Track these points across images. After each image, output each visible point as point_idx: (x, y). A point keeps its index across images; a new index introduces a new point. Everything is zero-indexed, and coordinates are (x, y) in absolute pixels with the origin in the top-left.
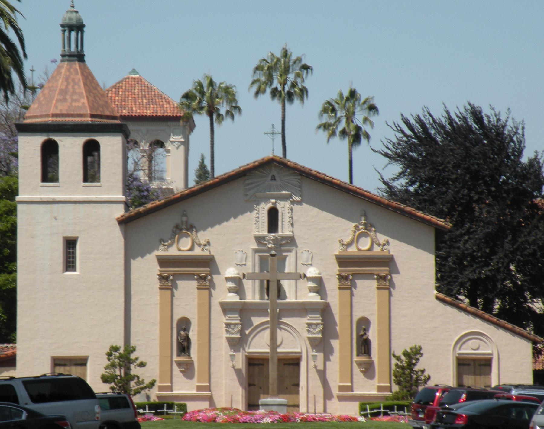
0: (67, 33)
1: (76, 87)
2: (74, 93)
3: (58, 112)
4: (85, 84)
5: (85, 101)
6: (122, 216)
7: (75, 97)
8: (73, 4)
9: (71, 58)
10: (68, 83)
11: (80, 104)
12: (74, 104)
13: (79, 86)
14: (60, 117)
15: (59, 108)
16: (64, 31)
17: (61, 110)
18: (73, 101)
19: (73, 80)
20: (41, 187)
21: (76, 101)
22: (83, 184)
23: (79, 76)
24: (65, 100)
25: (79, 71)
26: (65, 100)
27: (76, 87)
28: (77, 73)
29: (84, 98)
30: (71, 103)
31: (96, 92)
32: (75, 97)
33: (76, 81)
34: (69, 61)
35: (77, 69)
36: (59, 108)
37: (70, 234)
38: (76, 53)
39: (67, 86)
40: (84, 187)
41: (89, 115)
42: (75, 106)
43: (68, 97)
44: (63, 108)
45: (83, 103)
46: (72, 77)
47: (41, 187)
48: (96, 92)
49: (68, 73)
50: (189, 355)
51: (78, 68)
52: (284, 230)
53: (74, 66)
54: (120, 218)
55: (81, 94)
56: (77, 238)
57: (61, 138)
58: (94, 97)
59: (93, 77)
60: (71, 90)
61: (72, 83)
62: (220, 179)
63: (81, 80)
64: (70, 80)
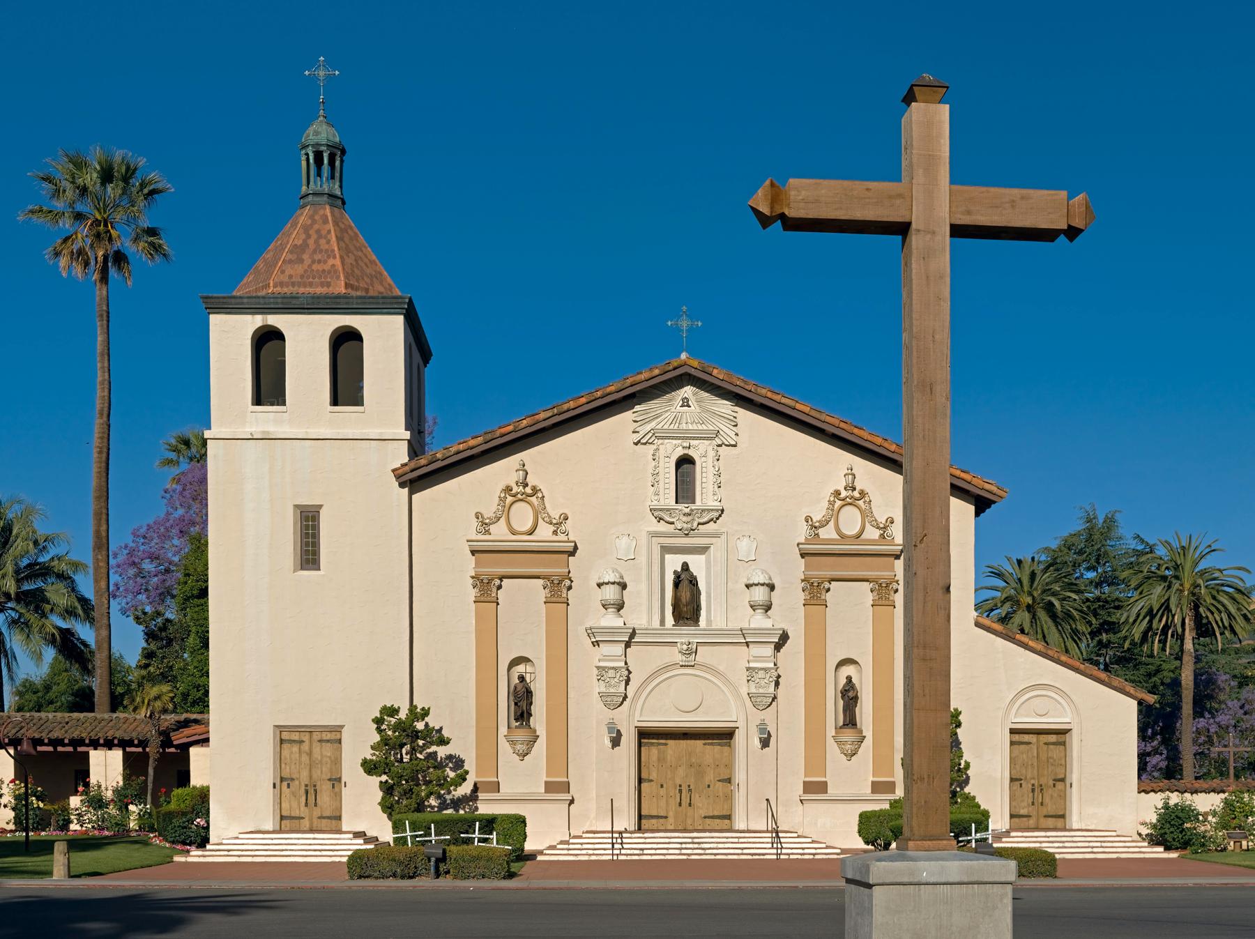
1: (323, 242)
4: (339, 239)
5: (338, 262)
10: (309, 236)
11: (327, 267)
12: (315, 267)
13: (328, 242)
18: (313, 262)
21: (319, 261)
23: (331, 226)
24: (301, 261)
25: (330, 218)
26: (301, 261)
27: (323, 242)
28: (325, 221)
29: (335, 257)
30: (310, 266)
31: (360, 253)
33: (324, 233)
35: (327, 216)
39: (305, 241)
43: (305, 257)
46: (316, 227)
48: (360, 253)
49: (309, 222)
51: (329, 214)
52: (705, 496)
53: (321, 212)
58: (356, 260)
61: (314, 236)
64: (311, 232)
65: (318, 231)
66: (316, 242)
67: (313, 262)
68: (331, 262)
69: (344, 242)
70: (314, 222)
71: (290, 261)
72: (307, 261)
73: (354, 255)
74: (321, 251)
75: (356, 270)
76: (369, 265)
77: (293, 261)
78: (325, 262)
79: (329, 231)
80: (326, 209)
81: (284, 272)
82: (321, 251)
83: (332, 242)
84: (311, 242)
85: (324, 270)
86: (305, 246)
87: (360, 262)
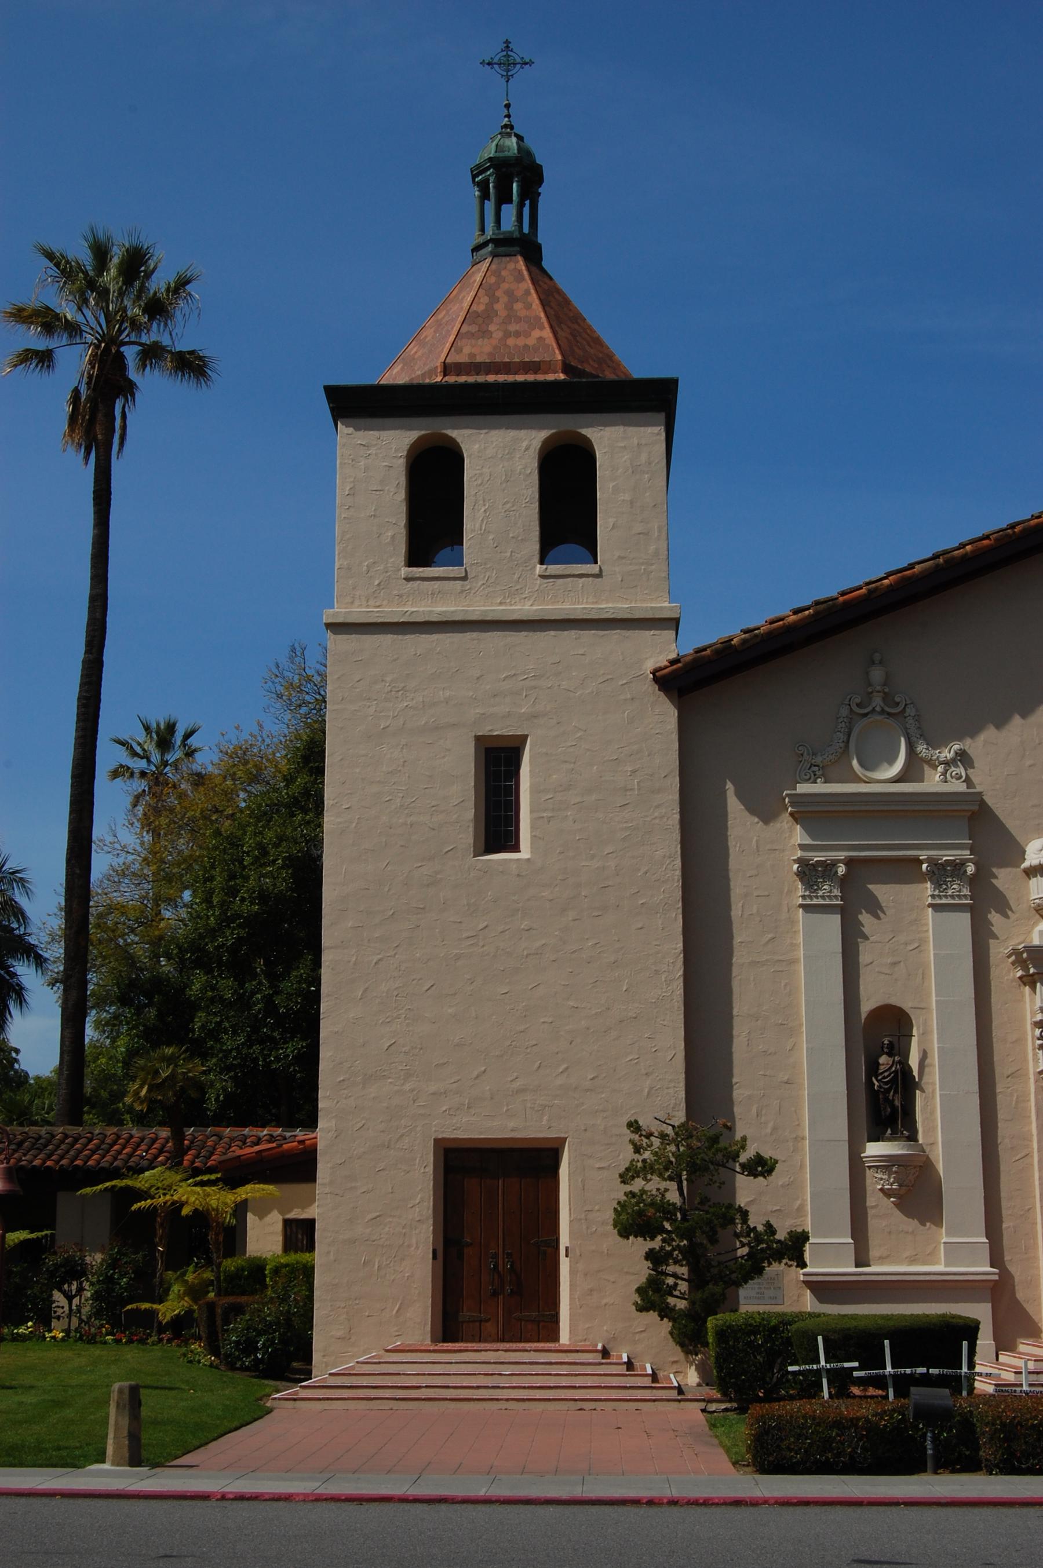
0: (490, 206)
1: (518, 306)
2: (509, 319)
3: (462, 358)
4: (544, 304)
5: (547, 333)
6: (673, 662)
7: (513, 328)
8: (510, 121)
9: (501, 250)
10: (494, 299)
11: (531, 341)
12: (511, 342)
13: (528, 307)
14: (468, 374)
15: (467, 350)
16: (483, 186)
17: (472, 355)
18: (507, 334)
19: (510, 293)
20: (408, 579)
21: (517, 334)
22: (539, 569)
23: (528, 284)
24: (485, 334)
25: (525, 273)
26: (485, 334)
27: (518, 306)
28: (520, 279)
29: (542, 328)
31: (576, 327)
32: (513, 328)
33: (519, 293)
34: (494, 255)
35: (520, 272)
36: (467, 350)
37: (501, 729)
38: (517, 235)
39: (490, 306)
40: (542, 577)
41: (559, 366)
42: (516, 346)
44: (480, 350)
45: (540, 339)
46: (505, 286)
47: (408, 579)
48: (576, 327)
50: (913, 1138)
51: (524, 268)
53: (511, 266)
54: (666, 667)
55: (535, 324)
56: (525, 738)
57: (467, 432)
59: (567, 302)
60: (502, 313)
61: (504, 299)
62: (996, 540)
63: (533, 291)
64: (498, 293)
65: (510, 293)
66: (509, 307)
67: (507, 334)
68: (536, 334)
69: (552, 308)
70: (501, 279)
71: (471, 335)
72: (498, 335)
73: (569, 327)
74: (519, 320)
75: (575, 349)
76: (592, 344)
77: (473, 335)
78: (528, 335)
79: (527, 293)
80: (518, 262)
81: (462, 351)
82: (519, 320)
83: (534, 306)
84: (499, 307)
85: (526, 346)
86: (488, 315)
87: (578, 338)
